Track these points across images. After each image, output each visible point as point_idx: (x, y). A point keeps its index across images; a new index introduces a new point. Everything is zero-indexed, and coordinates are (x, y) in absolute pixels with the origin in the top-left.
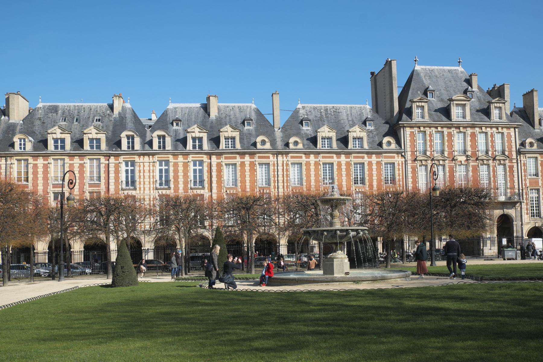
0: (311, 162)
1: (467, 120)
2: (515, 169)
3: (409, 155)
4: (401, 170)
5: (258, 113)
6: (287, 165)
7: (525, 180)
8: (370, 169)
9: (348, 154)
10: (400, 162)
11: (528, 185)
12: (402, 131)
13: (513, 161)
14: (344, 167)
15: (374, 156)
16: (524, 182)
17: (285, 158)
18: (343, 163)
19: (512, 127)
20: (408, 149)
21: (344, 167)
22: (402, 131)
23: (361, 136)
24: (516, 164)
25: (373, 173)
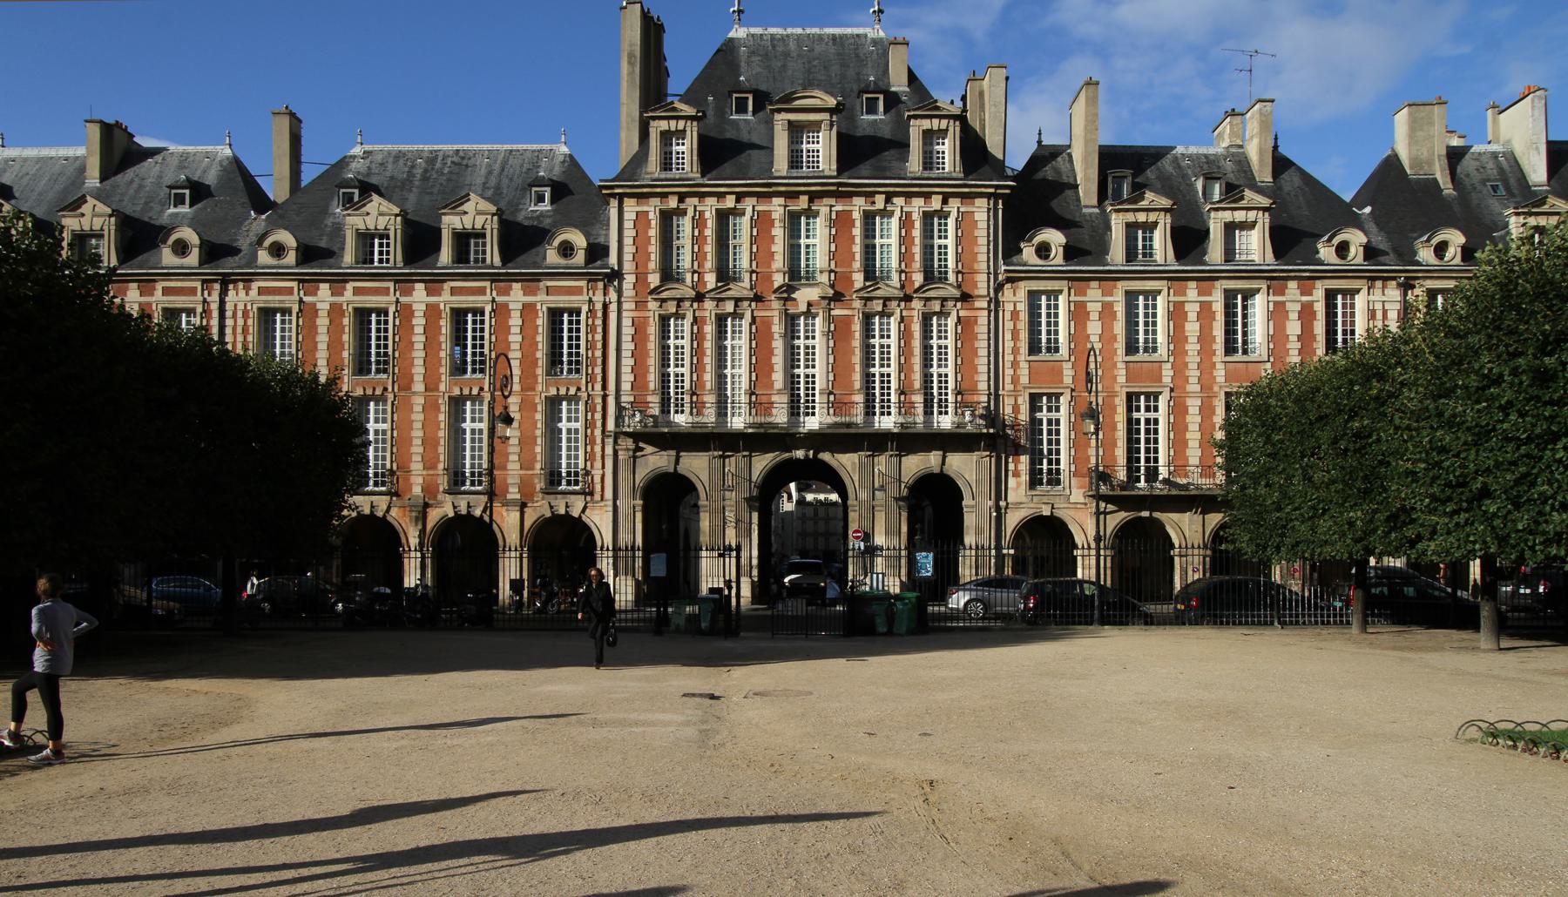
0: (319, 306)
1: (827, 173)
2: (982, 328)
3: (629, 280)
4: (599, 329)
5: (237, 164)
6: (245, 314)
7: (1015, 364)
8: (502, 329)
9: (434, 283)
10: (599, 306)
11: (1024, 380)
12: (613, 213)
13: (978, 304)
14: (419, 322)
15: (517, 286)
16: (1009, 372)
17: (242, 293)
18: (419, 309)
19: (981, 195)
20: (628, 266)
21: (419, 322)
22: (613, 213)
23: (478, 226)
24: (985, 313)
25: (511, 338)
